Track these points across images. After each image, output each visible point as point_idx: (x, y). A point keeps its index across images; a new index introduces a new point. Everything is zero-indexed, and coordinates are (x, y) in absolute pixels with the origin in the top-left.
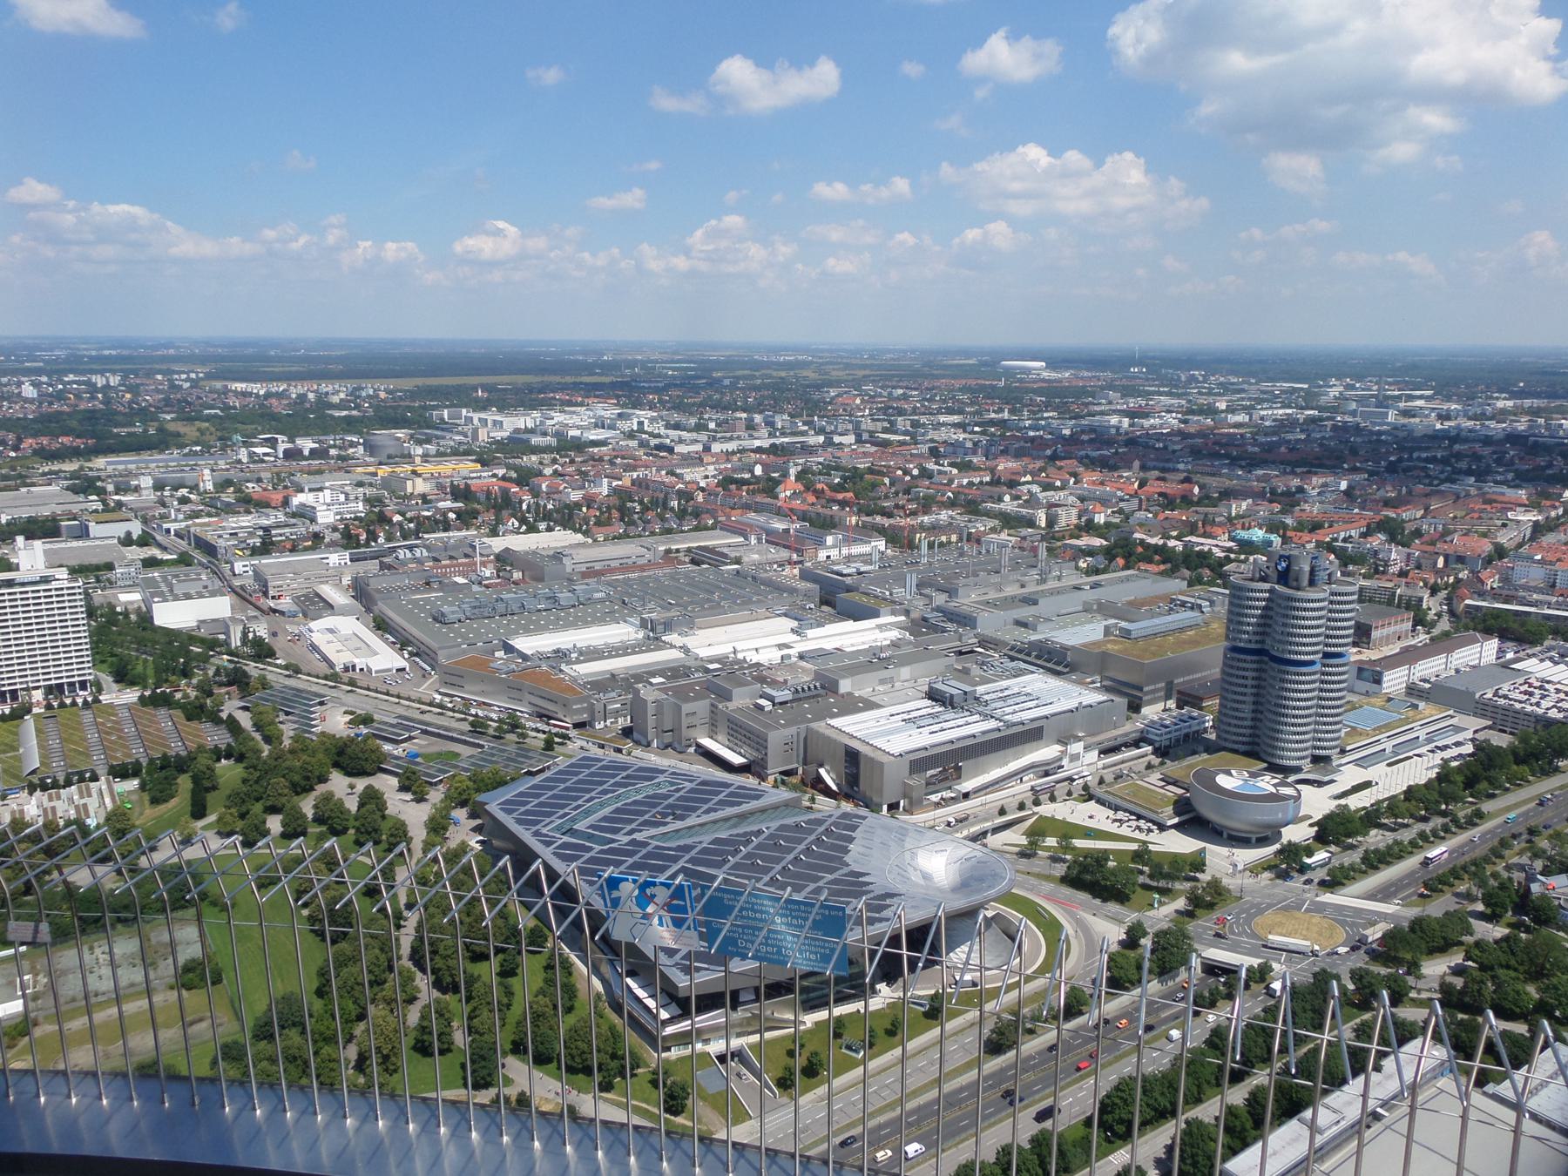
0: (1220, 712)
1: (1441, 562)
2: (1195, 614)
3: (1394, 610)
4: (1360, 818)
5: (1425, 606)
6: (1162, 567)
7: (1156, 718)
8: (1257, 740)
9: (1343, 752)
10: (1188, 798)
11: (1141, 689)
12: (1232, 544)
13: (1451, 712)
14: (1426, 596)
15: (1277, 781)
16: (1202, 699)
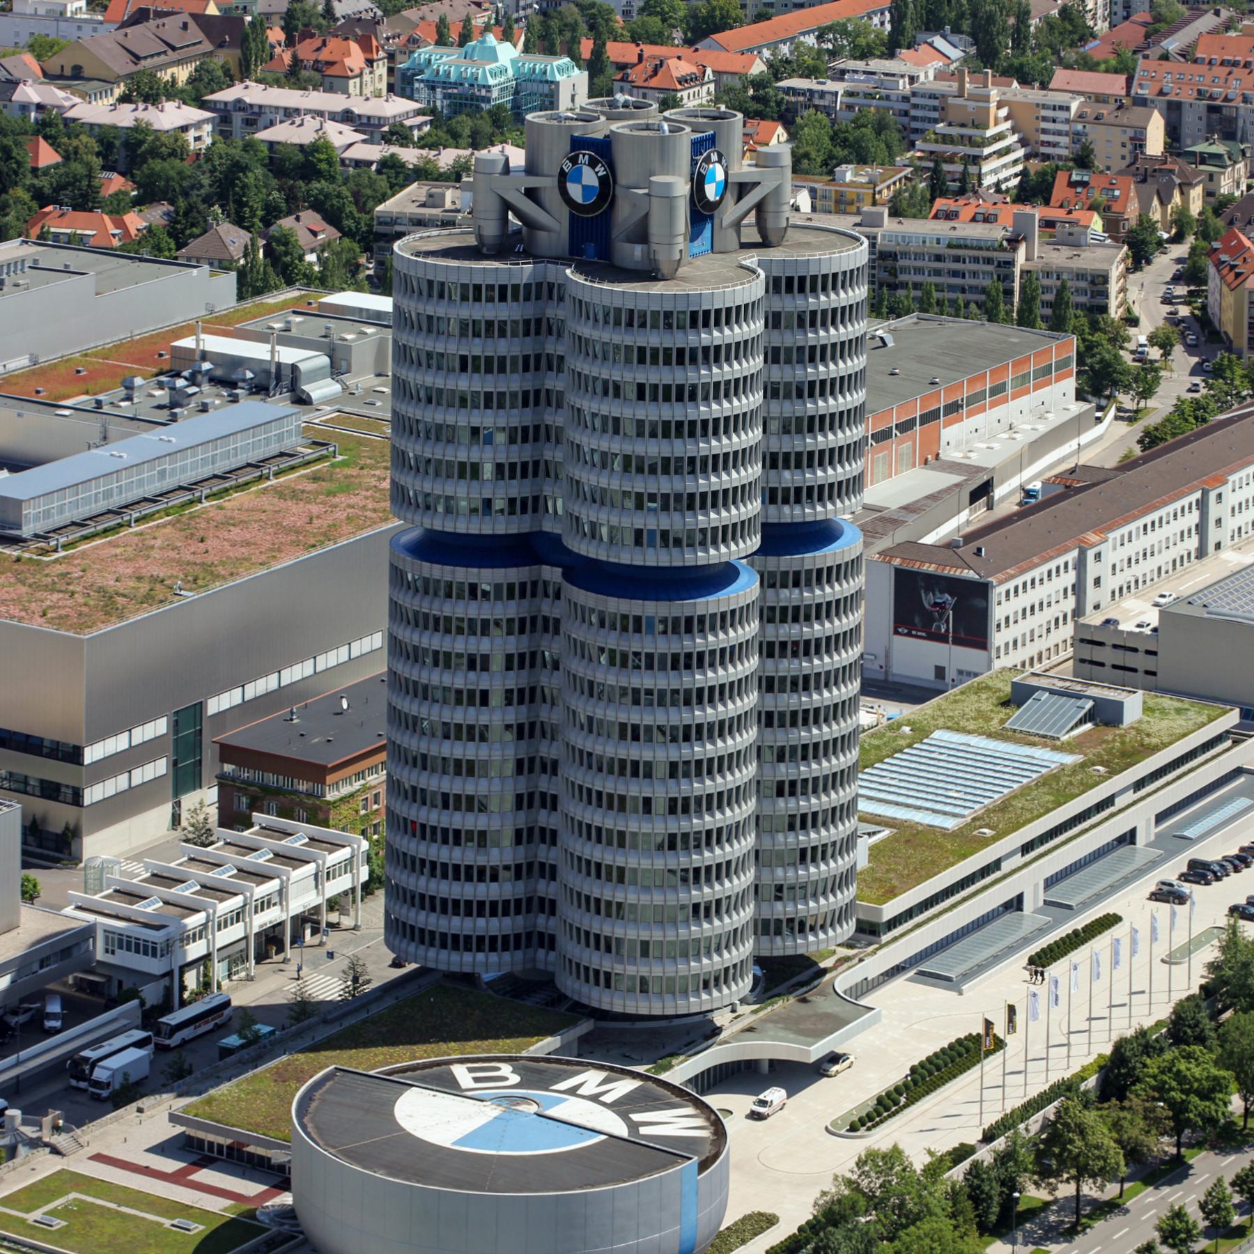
0: (394, 820)
1: (1155, 143)
2: (279, 405)
3: (1012, 335)
4: (954, 1195)
5: (1115, 312)
6: (135, 221)
7: (138, 874)
8: (542, 922)
9: (869, 931)
10: (288, 1214)
11: (75, 755)
12: (397, 107)
13: (1232, 718)
14: (1115, 271)
15: (625, 1086)
16: (318, 773)
